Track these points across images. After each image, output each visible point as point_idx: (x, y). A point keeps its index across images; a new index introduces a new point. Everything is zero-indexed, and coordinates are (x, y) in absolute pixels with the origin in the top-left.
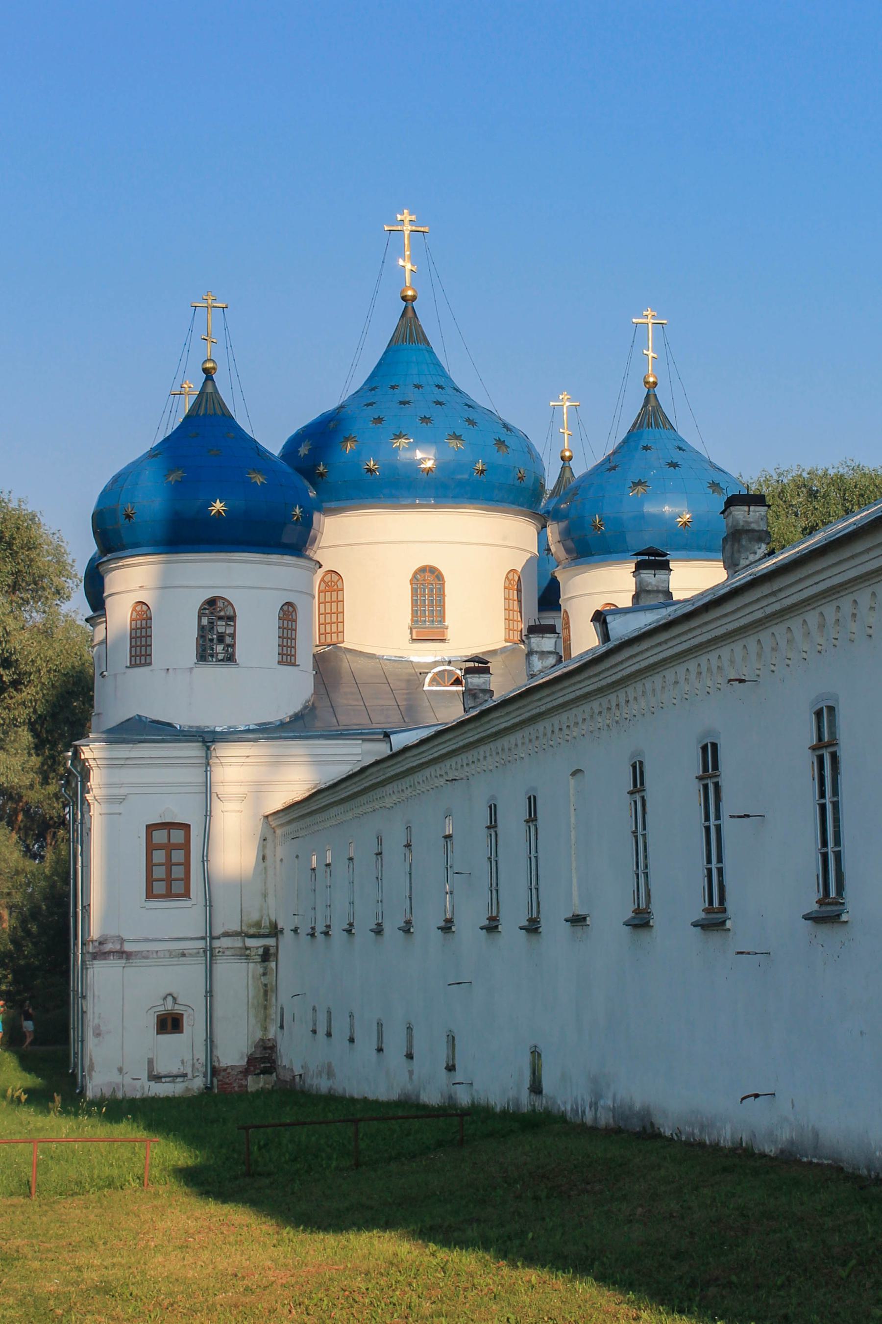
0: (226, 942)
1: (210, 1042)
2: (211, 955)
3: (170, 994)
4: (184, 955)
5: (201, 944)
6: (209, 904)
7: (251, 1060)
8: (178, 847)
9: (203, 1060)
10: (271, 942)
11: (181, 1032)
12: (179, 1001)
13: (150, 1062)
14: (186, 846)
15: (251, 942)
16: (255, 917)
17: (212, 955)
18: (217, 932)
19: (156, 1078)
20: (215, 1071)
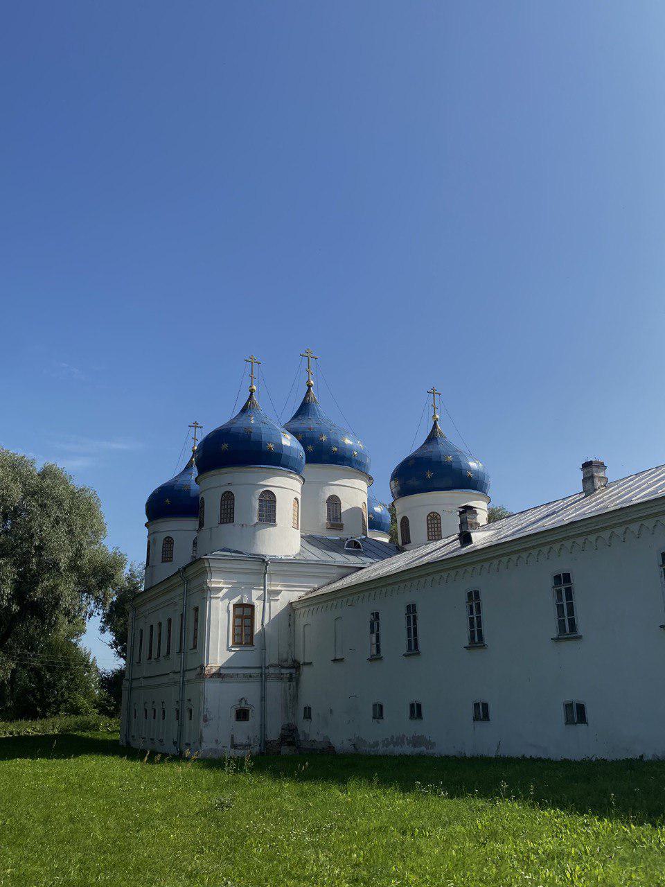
0: (271, 670)
1: (263, 726)
2: (263, 677)
3: (242, 699)
4: (250, 676)
5: (258, 671)
6: (264, 648)
7: (283, 737)
8: (246, 617)
9: (259, 736)
10: (292, 671)
11: (248, 720)
12: (248, 702)
13: (232, 738)
14: (252, 617)
15: (283, 671)
16: (285, 656)
17: (266, 678)
18: (267, 665)
19: (234, 746)
20: (266, 743)
